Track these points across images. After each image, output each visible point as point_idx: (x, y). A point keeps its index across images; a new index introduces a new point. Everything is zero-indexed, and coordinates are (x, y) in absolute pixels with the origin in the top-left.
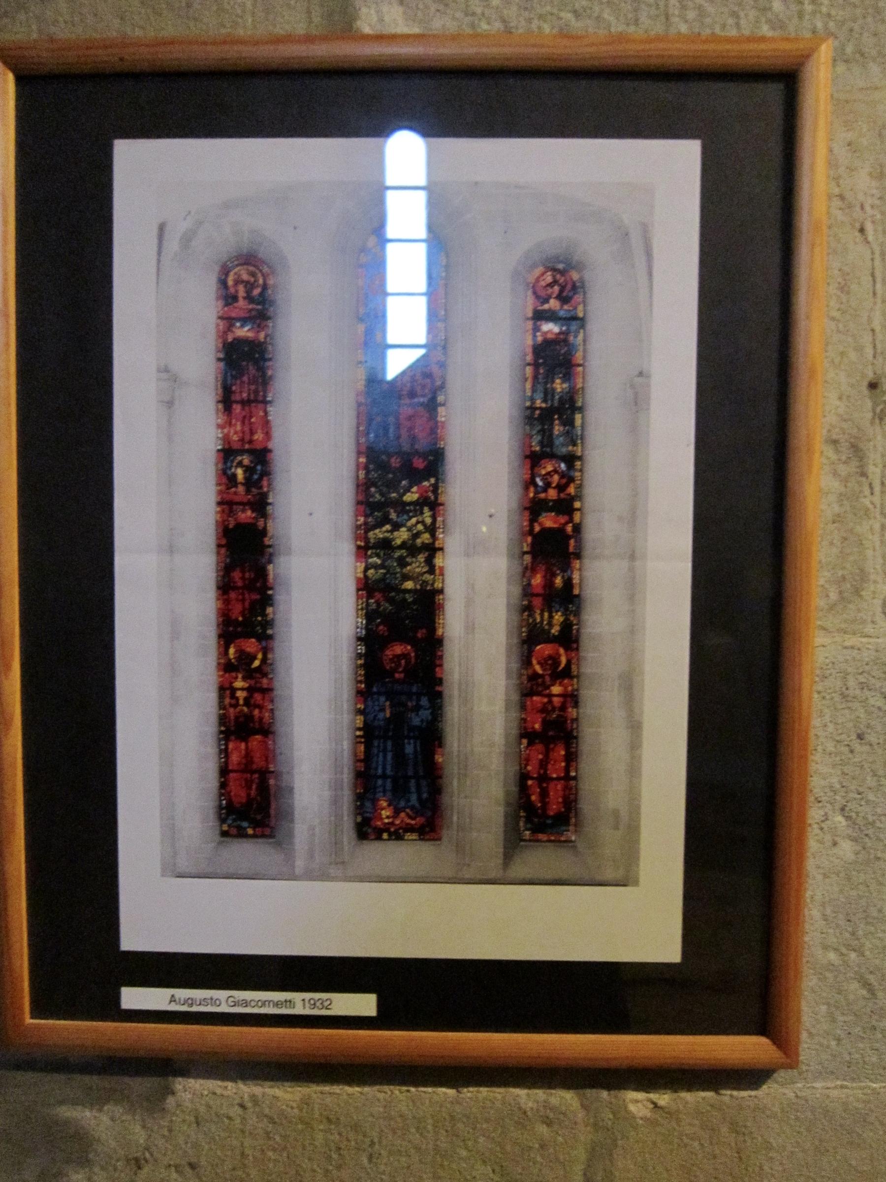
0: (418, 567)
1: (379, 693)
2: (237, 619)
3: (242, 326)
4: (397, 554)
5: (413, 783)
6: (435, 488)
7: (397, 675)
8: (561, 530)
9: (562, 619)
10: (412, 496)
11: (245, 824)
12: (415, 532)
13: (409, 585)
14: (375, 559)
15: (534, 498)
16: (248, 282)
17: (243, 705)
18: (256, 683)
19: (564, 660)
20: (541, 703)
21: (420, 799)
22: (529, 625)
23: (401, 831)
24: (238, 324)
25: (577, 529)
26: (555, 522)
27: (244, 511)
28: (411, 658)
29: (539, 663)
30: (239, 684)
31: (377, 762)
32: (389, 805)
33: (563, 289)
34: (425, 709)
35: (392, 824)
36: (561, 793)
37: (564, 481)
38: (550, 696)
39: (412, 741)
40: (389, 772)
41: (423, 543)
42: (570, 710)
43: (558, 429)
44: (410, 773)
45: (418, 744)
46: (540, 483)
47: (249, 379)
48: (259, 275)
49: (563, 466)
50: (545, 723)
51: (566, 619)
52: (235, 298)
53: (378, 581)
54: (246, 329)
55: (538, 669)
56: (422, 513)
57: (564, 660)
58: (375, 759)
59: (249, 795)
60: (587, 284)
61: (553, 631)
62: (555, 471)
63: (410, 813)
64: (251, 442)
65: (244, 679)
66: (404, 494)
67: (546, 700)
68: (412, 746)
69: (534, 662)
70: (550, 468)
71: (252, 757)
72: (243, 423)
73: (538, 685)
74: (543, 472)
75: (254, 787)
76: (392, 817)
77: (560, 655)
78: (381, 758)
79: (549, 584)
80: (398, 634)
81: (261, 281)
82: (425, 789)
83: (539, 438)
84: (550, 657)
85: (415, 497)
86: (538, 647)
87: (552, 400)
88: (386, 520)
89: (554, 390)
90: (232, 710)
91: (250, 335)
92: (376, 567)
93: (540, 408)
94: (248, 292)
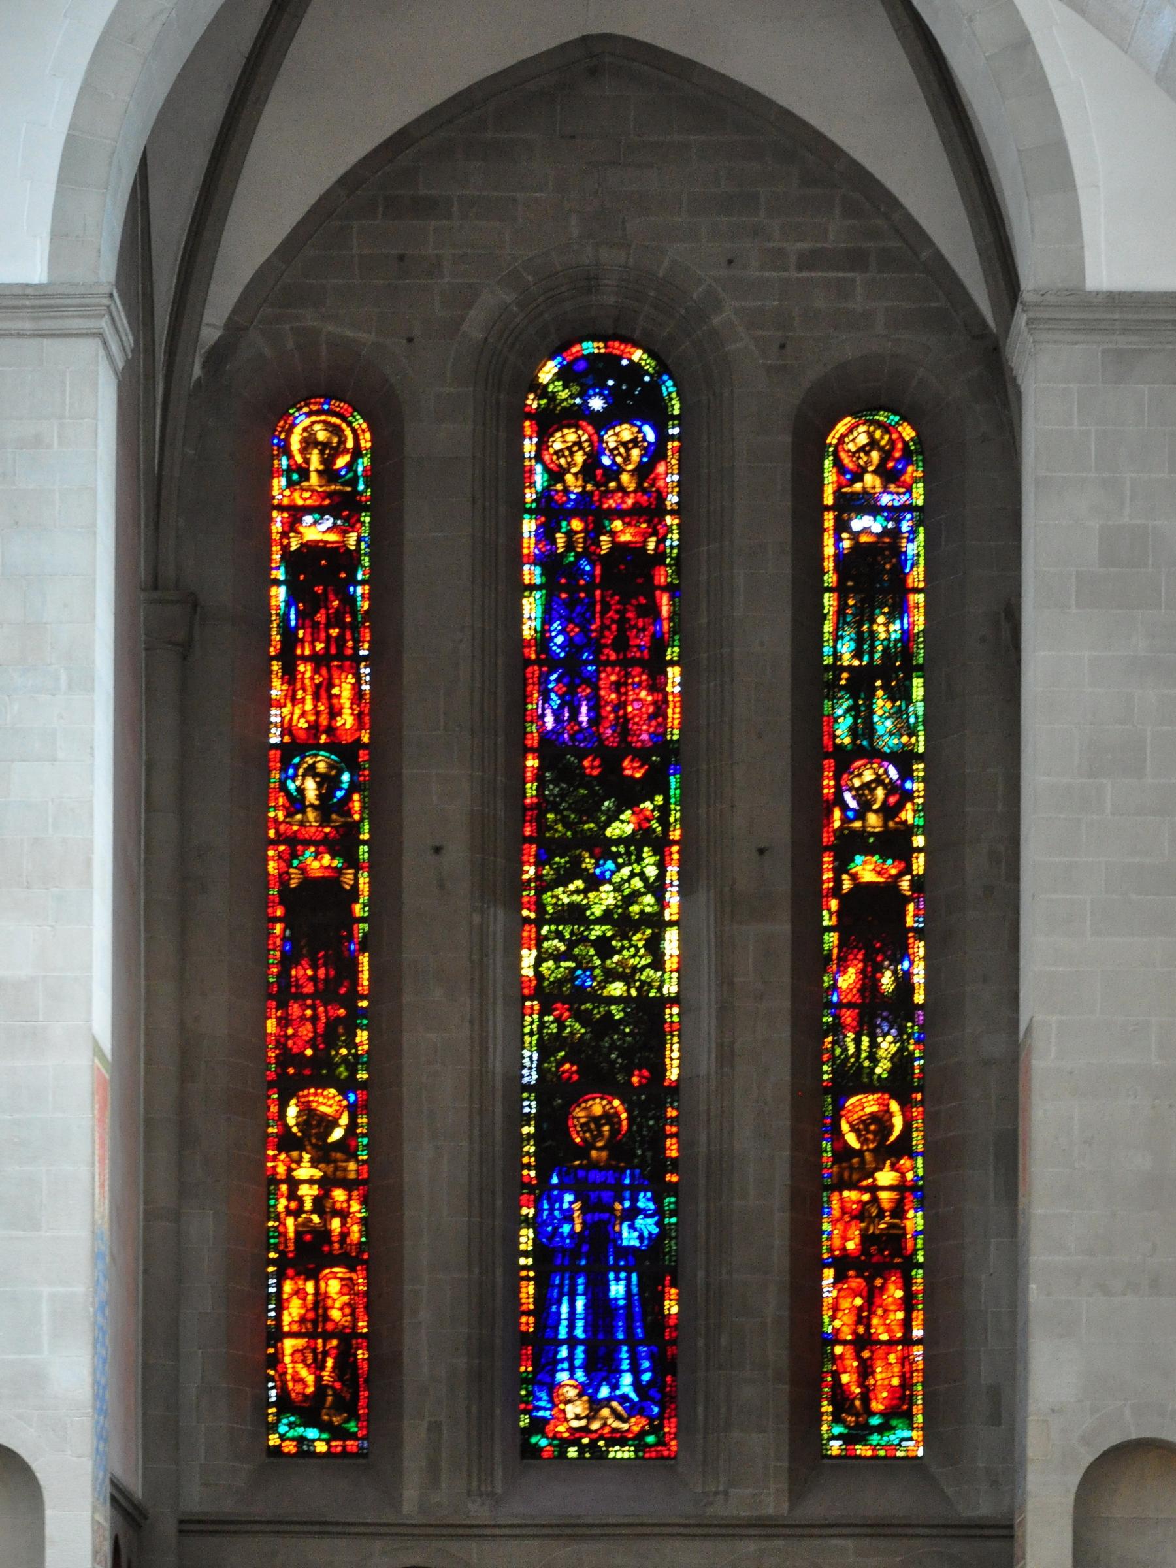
0: (634, 956)
1: (563, 1188)
4: (597, 932)
7: (594, 1153)
8: (892, 885)
9: (894, 1048)
11: (312, 1433)
12: (626, 892)
13: (617, 989)
14: (556, 942)
15: (841, 828)
16: (325, 445)
17: (312, 1212)
18: (336, 1169)
19: (898, 1122)
20: (859, 1202)
21: (637, 1384)
23: (601, 1443)
26: (879, 873)
27: (317, 856)
28: (620, 1121)
29: (853, 1129)
30: (305, 1171)
31: (558, 1313)
32: (580, 1395)
34: (647, 1216)
35: (585, 1430)
38: (874, 1189)
39: (623, 1275)
40: (579, 1333)
41: (642, 912)
42: (911, 1214)
43: (881, 704)
45: (634, 1277)
46: (853, 804)
48: (348, 432)
49: (893, 773)
50: (866, 1239)
51: (900, 1050)
52: (304, 474)
53: (560, 982)
55: (852, 1140)
56: (640, 859)
57: (898, 1122)
58: (554, 1308)
59: (318, 1379)
61: (878, 1070)
62: (878, 781)
63: (620, 1408)
64: (331, 730)
65: (314, 1163)
66: (608, 824)
67: (866, 1197)
68: (623, 1283)
69: (845, 1127)
70: (868, 776)
71: (326, 1309)
72: (316, 698)
73: (851, 1168)
74: (857, 783)
75: (330, 1363)
76: (586, 1417)
77: (891, 1115)
78: (565, 1309)
79: (869, 982)
80: (599, 1080)
81: (350, 444)
83: (849, 720)
84: (873, 1117)
85: (628, 829)
86: (853, 1100)
87: (872, 653)
88: (574, 871)
90: (290, 1222)
91: (332, 537)
92: (558, 957)
93: (850, 668)
94: (328, 462)
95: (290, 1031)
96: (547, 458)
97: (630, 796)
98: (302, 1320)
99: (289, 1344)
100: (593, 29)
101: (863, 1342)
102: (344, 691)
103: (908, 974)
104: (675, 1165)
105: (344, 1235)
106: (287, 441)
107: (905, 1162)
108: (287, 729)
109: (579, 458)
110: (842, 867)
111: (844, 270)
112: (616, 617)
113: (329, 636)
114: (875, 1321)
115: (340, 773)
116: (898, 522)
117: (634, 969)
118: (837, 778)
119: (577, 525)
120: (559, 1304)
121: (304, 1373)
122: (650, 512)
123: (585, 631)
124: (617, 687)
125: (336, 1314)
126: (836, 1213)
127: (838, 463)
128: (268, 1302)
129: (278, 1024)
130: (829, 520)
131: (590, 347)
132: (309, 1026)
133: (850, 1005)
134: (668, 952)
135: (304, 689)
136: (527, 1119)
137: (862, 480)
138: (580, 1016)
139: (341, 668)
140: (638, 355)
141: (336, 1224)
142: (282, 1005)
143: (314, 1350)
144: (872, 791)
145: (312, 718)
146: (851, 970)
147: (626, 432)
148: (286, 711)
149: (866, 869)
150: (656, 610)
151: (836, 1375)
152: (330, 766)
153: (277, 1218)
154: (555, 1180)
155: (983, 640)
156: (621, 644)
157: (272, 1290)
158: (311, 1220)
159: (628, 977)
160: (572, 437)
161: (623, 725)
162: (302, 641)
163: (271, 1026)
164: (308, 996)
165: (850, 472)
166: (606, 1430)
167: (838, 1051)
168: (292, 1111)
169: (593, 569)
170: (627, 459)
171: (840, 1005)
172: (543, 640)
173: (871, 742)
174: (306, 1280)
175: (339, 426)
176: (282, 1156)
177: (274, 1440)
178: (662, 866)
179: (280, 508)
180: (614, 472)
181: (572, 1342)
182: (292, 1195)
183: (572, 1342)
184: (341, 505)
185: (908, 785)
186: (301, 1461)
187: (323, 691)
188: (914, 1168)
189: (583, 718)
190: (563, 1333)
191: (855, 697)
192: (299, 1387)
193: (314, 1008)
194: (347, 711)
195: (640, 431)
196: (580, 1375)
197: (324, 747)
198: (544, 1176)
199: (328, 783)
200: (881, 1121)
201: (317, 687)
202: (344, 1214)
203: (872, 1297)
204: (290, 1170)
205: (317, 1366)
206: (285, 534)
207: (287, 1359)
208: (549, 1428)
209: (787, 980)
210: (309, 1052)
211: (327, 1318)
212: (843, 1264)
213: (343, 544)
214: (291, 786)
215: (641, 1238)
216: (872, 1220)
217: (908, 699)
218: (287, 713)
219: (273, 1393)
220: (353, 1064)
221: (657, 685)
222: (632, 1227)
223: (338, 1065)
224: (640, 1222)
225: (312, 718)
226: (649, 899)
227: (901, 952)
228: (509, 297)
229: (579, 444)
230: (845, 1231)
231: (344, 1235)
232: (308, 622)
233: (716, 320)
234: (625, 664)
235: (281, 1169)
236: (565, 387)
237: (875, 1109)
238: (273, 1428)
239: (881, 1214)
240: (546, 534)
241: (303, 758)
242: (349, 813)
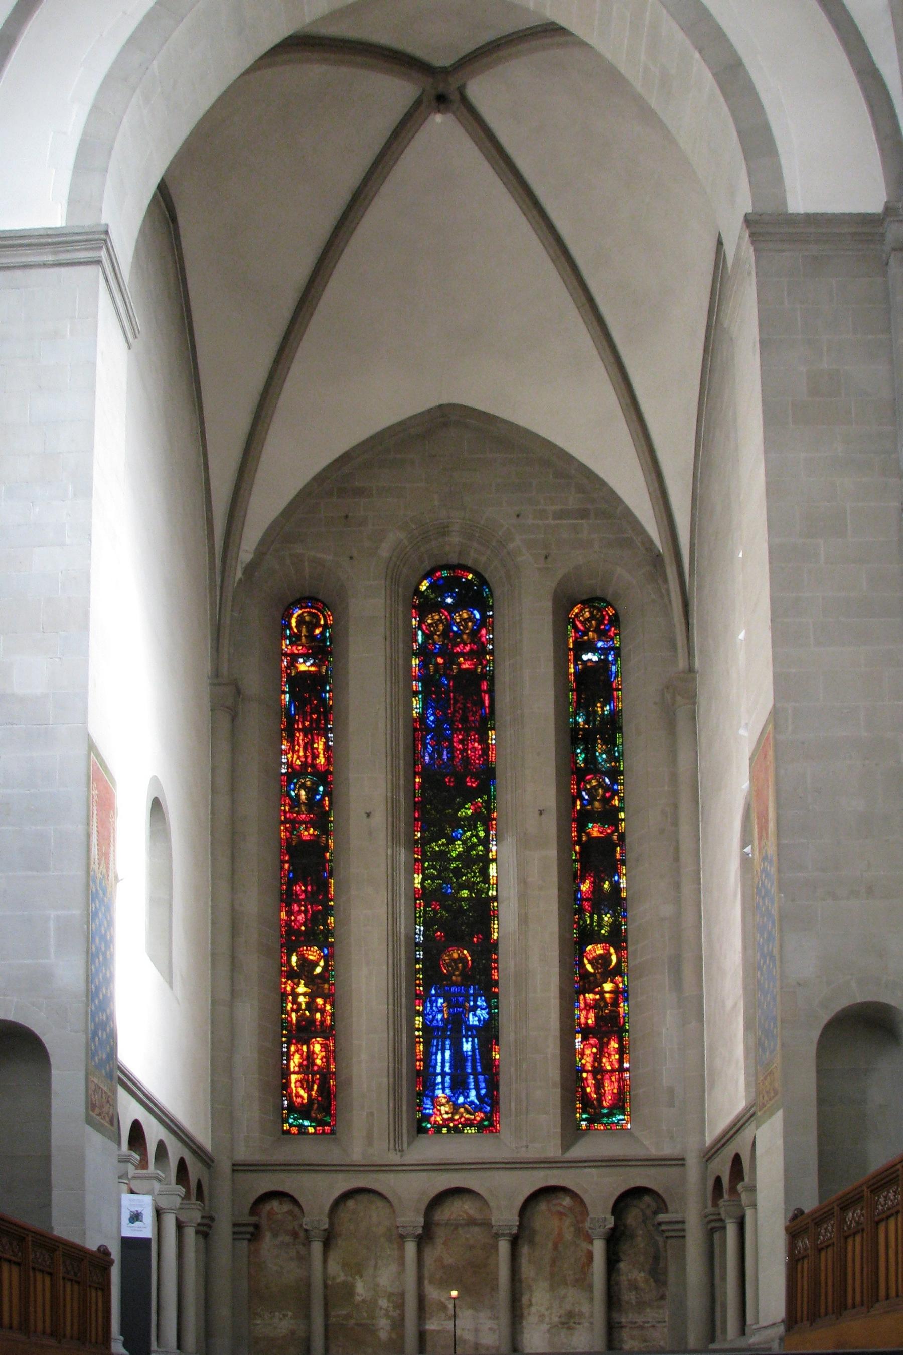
1: (438, 996)
2: (299, 929)
3: (304, 662)
5: (471, 1079)
6: (488, 803)
7: (454, 978)
11: (306, 1123)
13: (465, 893)
17: (305, 1010)
18: (318, 987)
19: (614, 958)
20: (595, 1000)
21: (478, 1095)
22: (579, 926)
24: (301, 660)
25: (622, 837)
27: (306, 829)
29: (590, 962)
30: (301, 989)
31: (436, 1060)
32: (448, 1102)
33: (600, 622)
34: (482, 1009)
36: (616, 1085)
37: (607, 795)
38: (602, 993)
39: (470, 1039)
40: (447, 1070)
42: (621, 1005)
44: (469, 1071)
45: (476, 1040)
47: (311, 709)
48: (321, 616)
52: (298, 637)
53: (436, 890)
54: (308, 664)
55: (589, 967)
56: (476, 828)
57: (614, 958)
58: (434, 1057)
59: (309, 1096)
60: (621, 619)
61: (603, 932)
62: (600, 785)
64: (313, 766)
65: (306, 985)
67: (598, 997)
68: (470, 1043)
69: (586, 961)
70: (594, 783)
71: (314, 1060)
72: (305, 750)
75: (315, 1087)
77: (611, 954)
78: (439, 1057)
79: (597, 887)
81: (322, 622)
82: (483, 1085)
86: (590, 947)
87: (595, 720)
89: (596, 712)
91: (312, 669)
92: (433, 878)
94: (311, 631)
95: (293, 918)
96: (424, 627)
97: (469, 796)
98: (300, 1065)
99: (294, 1078)
100: (445, 400)
101: (598, 1071)
102: (320, 745)
103: (618, 883)
105: (323, 1021)
106: (290, 623)
107: (618, 979)
108: (290, 765)
109: (441, 627)
110: (582, 828)
111: (576, 519)
112: (462, 706)
113: (311, 718)
114: (604, 1060)
115: (318, 786)
116: (607, 655)
117: (474, 883)
118: (578, 784)
119: (440, 661)
120: (436, 1054)
121: (302, 1092)
122: (479, 653)
123: (445, 714)
124: (461, 742)
125: (318, 1062)
126: (582, 1005)
127: (575, 627)
128: (283, 1056)
129: (287, 915)
131: (445, 573)
132: (303, 915)
133: (587, 900)
134: (491, 874)
135: (299, 745)
136: (418, 961)
137: (587, 635)
138: (444, 907)
139: (318, 735)
140: (470, 576)
141: (318, 1016)
142: (289, 905)
143: (307, 1081)
144: (597, 790)
145: (303, 760)
146: (588, 881)
148: (289, 756)
149: (595, 830)
150: (483, 702)
151: (584, 1089)
152: (312, 783)
153: (287, 1013)
154: (433, 992)
155: (655, 703)
156: (464, 720)
157: (285, 1050)
158: (304, 1014)
159: (470, 886)
160: (437, 617)
161: (466, 760)
162: (298, 721)
163: (283, 915)
164: (303, 900)
165: (581, 631)
166: (463, 1119)
167: (581, 923)
168: (294, 959)
169: (449, 682)
170: (466, 627)
171: (582, 899)
172: (423, 717)
173: (595, 767)
174: (302, 1045)
175: (316, 614)
176: (290, 982)
177: (286, 1127)
178: (487, 831)
179: (286, 655)
180: (458, 635)
181: (443, 1074)
182: (295, 1001)
183: (443, 1074)
185: (615, 787)
186: (299, 1136)
187: (309, 746)
188: (623, 982)
189: (445, 757)
190: (439, 1070)
191: (586, 744)
192: (299, 1100)
193: (305, 906)
194: (321, 755)
195: (472, 613)
196: (448, 1091)
197: (310, 774)
198: (427, 990)
199: (312, 792)
200: (606, 957)
201: (305, 744)
202: (322, 1011)
203: (602, 1049)
204: (293, 989)
205: (309, 1089)
206: (288, 668)
207: (293, 1085)
208: (433, 1119)
209: (555, 879)
210: (303, 928)
211: (314, 1064)
212: (587, 1032)
213: (319, 671)
214: (293, 794)
215: (479, 1020)
216: (601, 1008)
217: (615, 745)
219: (286, 1102)
222: (475, 1015)
223: (319, 934)
224: (478, 1012)
225: (303, 760)
226: (480, 848)
227: (616, 871)
228: (402, 535)
229: (440, 620)
230: (587, 1014)
231: (323, 1021)
232: (301, 712)
233: (511, 546)
234: (467, 731)
235: (289, 988)
236: (432, 593)
237: (601, 951)
238: (285, 1120)
239: (606, 1004)
240: (424, 666)
241: (298, 781)
242: (323, 806)
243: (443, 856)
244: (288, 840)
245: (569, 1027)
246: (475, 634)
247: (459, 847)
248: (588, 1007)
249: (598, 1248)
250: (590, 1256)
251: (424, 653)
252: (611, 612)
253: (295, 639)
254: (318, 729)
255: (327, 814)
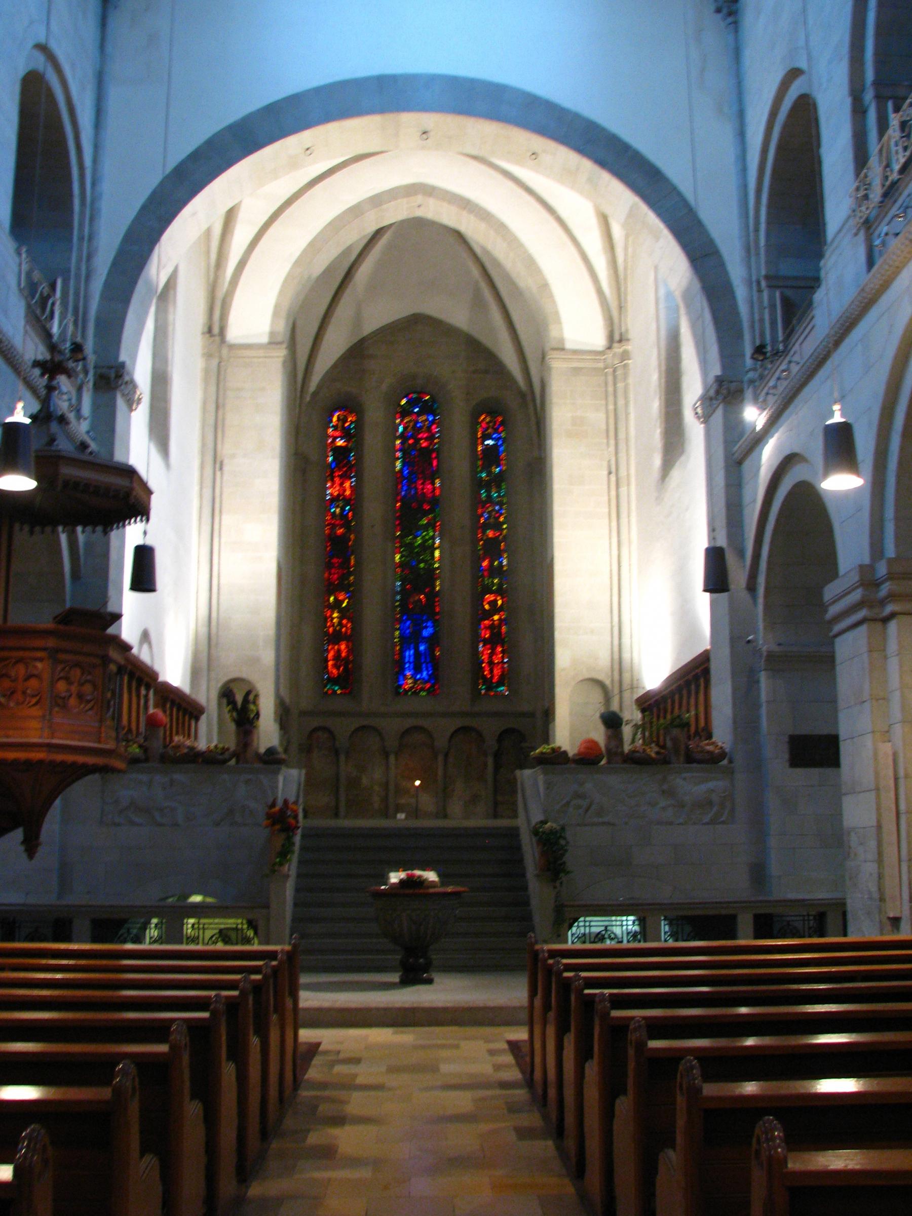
1: (407, 620)
10: (424, 521)
19: (500, 602)
55: (487, 607)
70: (490, 509)
97: (425, 514)
98: (334, 656)
99: (330, 663)
101: (491, 663)
104: (438, 613)
105: (346, 632)
110: (484, 533)
122: (431, 438)
125: (343, 655)
130: (479, 441)
147: (424, 418)
149: (490, 533)
168: (332, 599)
172: (401, 471)
180: (421, 427)
184: (346, 434)
187: (341, 484)
199: (343, 509)
200: (496, 601)
202: (346, 626)
205: (338, 669)
212: (486, 642)
218: (331, 491)
220: (350, 585)
221: (433, 483)
243: (410, 546)
244: (329, 535)
245: (476, 638)
246: (429, 429)
247: (419, 541)
248: (486, 628)
249: (490, 761)
250: (485, 764)
251: (403, 436)
252: (500, 419)
253: (335, 428)
254: (345, 477)
255: (351, 521)
